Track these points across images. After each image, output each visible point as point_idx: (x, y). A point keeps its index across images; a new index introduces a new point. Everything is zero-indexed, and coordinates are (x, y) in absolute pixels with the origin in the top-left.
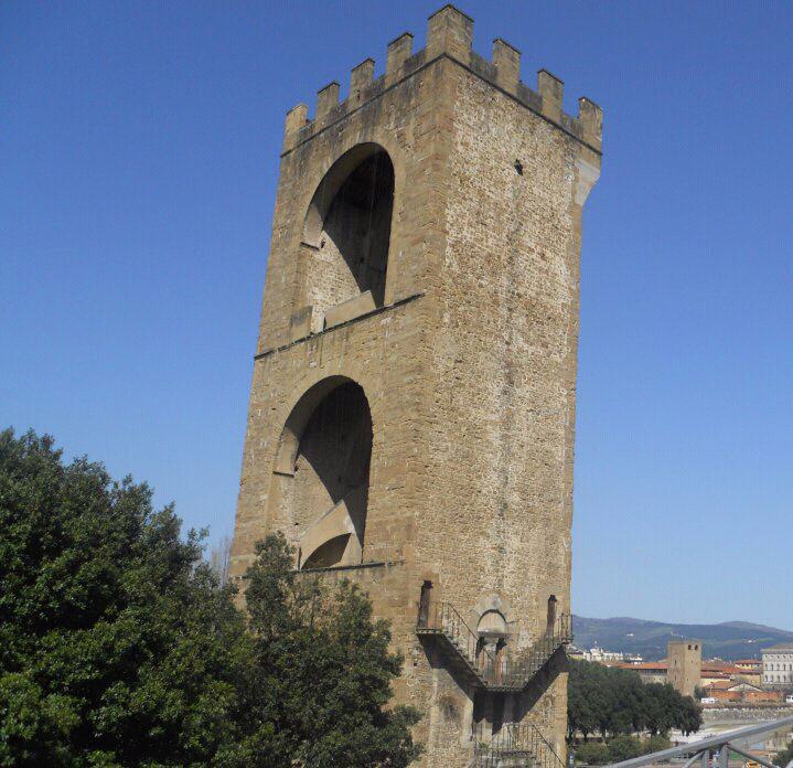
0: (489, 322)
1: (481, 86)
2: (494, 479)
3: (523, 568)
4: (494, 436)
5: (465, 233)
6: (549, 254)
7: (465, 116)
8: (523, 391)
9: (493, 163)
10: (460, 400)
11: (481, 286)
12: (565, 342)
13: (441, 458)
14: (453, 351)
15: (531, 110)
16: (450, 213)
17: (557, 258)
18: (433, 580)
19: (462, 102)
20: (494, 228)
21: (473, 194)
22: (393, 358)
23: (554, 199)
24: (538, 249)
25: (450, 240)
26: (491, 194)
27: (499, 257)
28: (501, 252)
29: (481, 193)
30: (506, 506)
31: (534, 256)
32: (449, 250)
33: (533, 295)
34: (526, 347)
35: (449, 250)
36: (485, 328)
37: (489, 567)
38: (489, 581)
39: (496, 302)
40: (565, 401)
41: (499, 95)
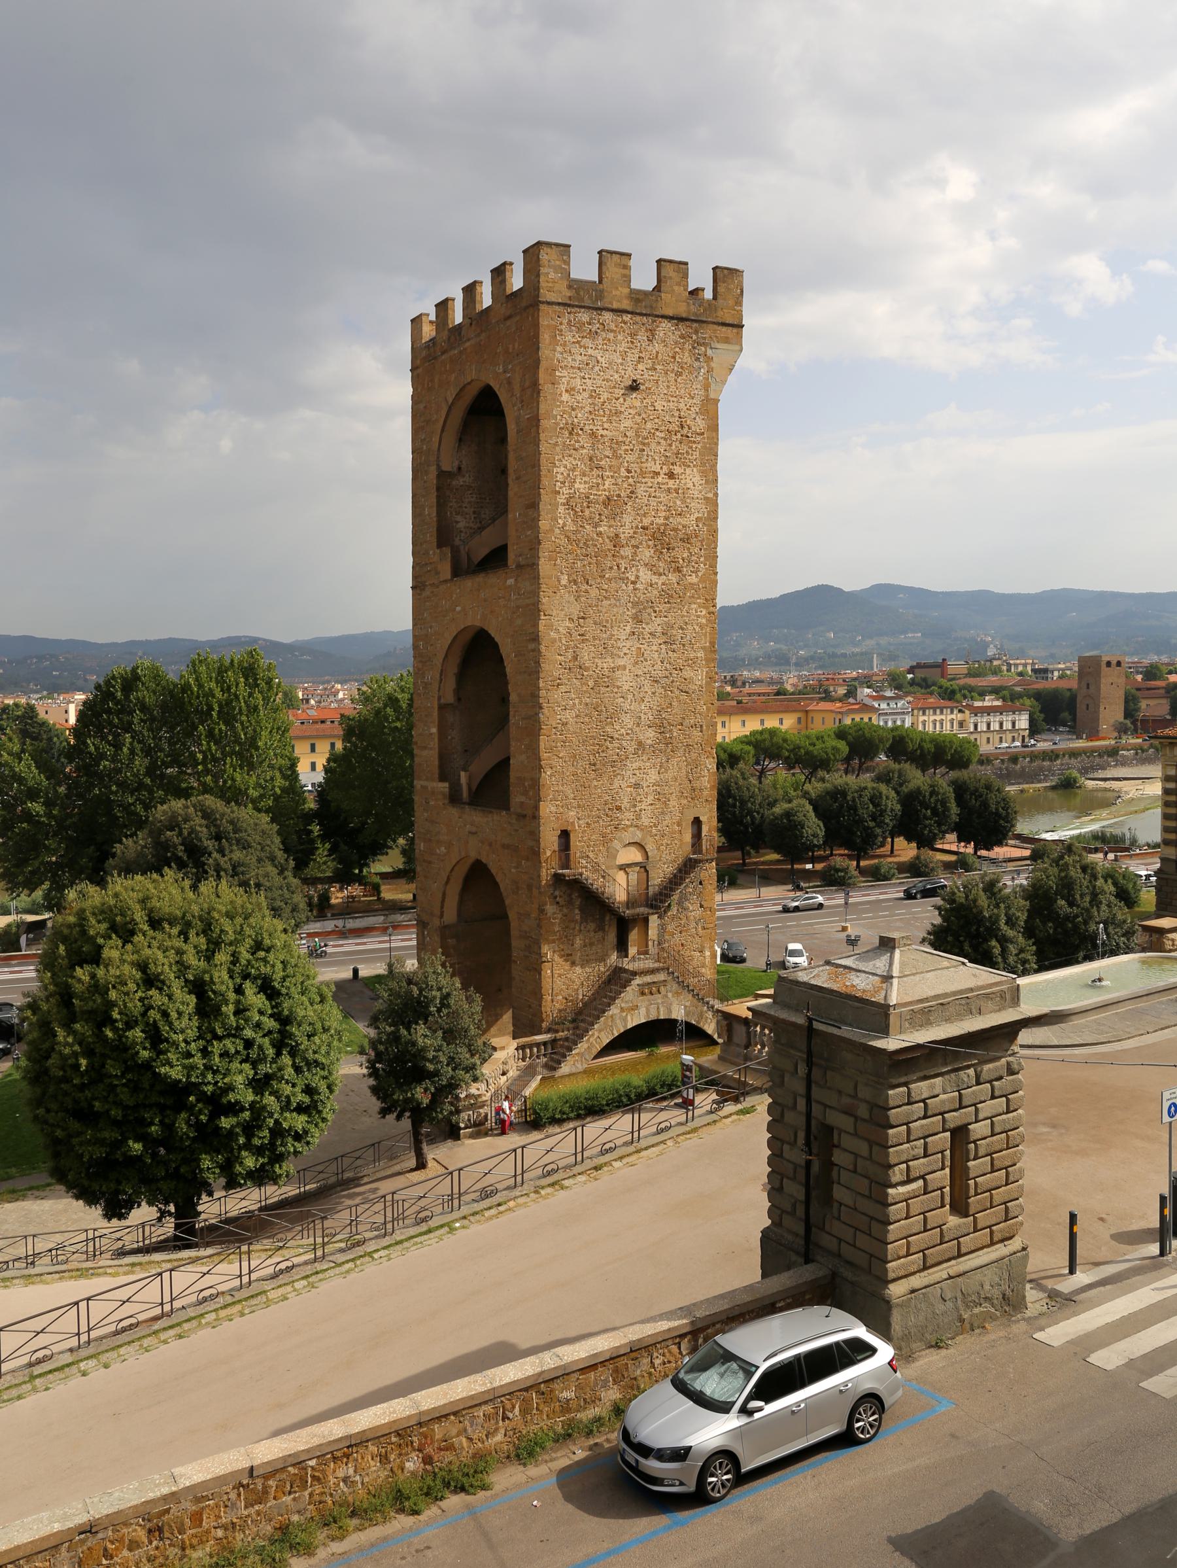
0: (611, 568)
1: (584, 316)
2: (628, 721)
3: (661, 798)
4: (625, 680)
5: (576, 486)
6: (677, 470)
7: (570, 359)
8: (656, 625)
9: (605, 396)
10: (586, 656)
11: (600, 534)
13: (569, 716)
14: (575, 610)
15: (645, 315)
17: (688, 471)
18: (569, 828)
19: (564, 345)
20: (610, 467)
21: (584, 440)
22: (519, 622)
23: (682, 406)
25: (561, 499)
27: (619, 496)
29: (593, 434)
30: (640, 744)
32: (561, 509)
33: (662, 521)
34: (655, 579)
35: (561, 509)
37: (625, 804)
38: (627, 817)
40: (704, 621)
41: (607, 316)
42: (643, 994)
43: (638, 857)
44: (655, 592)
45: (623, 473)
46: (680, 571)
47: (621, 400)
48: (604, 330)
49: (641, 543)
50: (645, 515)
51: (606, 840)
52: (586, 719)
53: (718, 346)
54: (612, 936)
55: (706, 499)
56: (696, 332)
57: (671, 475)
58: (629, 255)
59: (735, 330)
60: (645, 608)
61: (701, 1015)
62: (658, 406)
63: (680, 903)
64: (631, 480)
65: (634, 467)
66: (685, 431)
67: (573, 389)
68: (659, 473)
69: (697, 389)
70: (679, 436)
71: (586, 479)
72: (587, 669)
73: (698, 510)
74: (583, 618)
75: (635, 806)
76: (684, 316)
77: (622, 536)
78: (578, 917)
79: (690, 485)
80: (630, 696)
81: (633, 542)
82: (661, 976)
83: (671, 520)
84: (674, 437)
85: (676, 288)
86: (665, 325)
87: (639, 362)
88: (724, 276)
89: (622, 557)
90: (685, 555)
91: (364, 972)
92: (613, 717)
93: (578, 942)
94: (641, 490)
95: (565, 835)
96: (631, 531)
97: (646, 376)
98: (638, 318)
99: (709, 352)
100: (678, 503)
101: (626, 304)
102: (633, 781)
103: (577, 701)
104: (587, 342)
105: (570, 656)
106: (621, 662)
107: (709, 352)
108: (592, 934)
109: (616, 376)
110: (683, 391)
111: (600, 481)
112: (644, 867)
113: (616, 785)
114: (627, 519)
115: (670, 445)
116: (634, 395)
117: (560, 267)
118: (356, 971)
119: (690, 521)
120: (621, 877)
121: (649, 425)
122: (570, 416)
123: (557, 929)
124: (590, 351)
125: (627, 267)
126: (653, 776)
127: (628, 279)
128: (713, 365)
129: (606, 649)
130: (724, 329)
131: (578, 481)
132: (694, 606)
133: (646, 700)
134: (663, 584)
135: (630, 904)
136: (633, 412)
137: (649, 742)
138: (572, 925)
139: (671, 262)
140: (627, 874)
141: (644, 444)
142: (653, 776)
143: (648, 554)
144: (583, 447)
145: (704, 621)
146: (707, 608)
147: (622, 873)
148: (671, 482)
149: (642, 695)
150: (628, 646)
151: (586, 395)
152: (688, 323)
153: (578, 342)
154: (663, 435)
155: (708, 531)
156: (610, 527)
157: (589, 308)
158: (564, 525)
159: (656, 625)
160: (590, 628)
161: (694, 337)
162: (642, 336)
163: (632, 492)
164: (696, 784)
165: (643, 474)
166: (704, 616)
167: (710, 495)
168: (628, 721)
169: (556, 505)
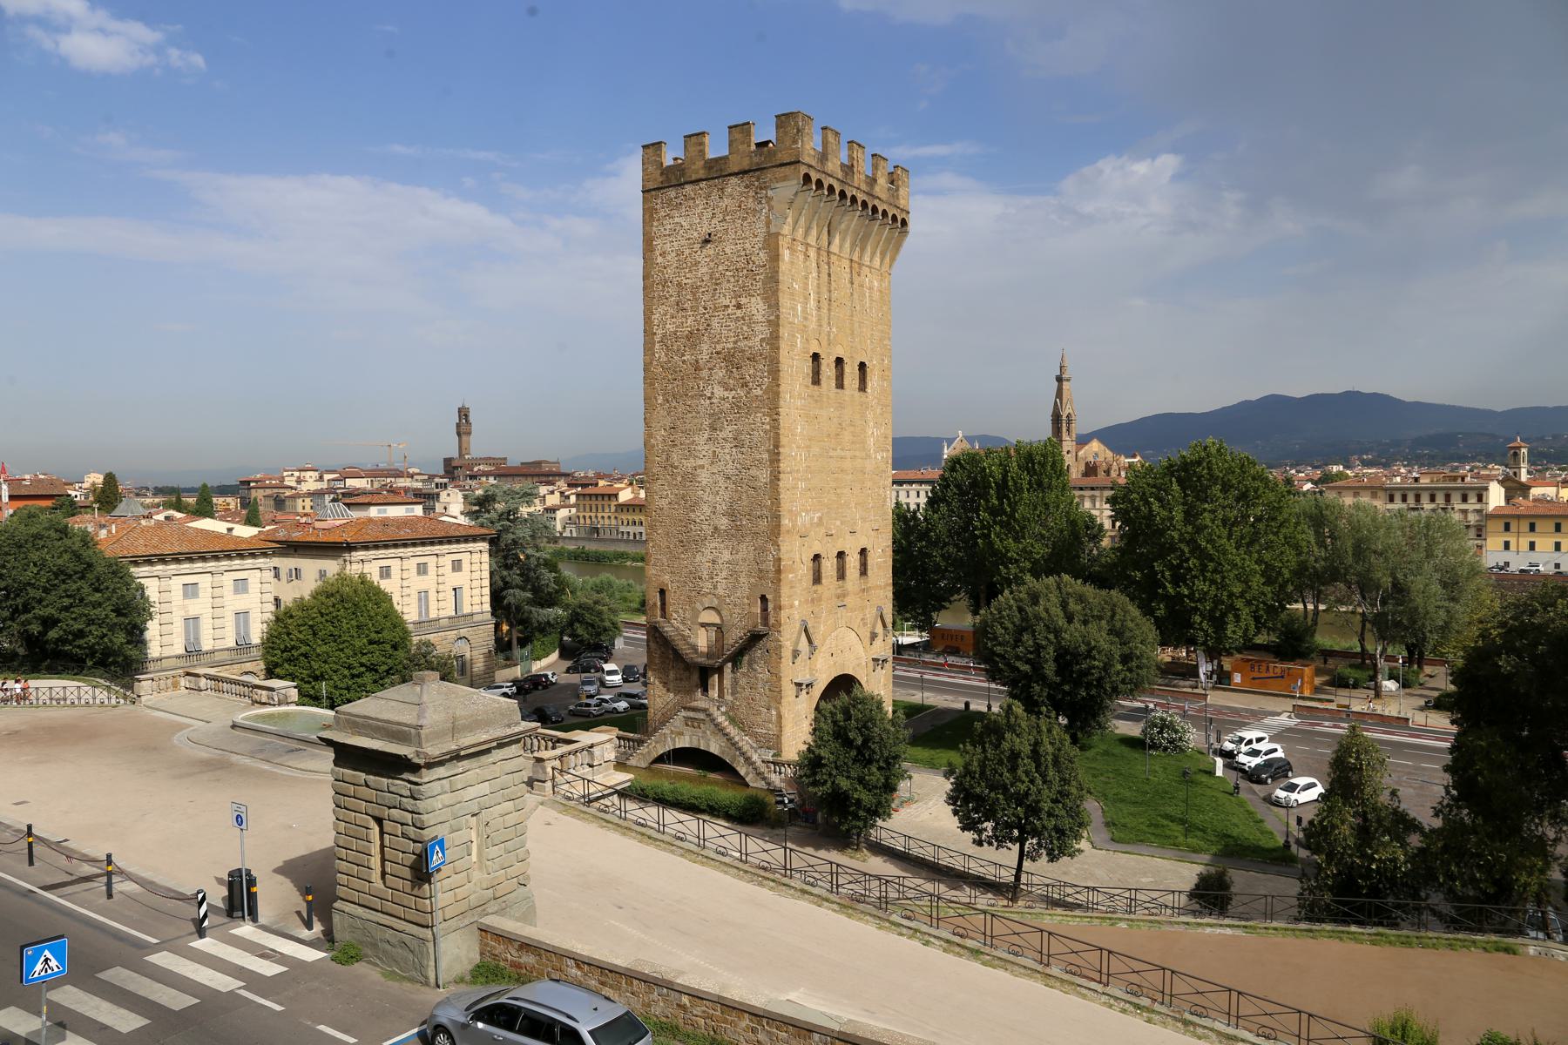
1: (672, 193)
2: (706, 509)
3: (734, 574)
4: (704, 477)
6: (743, 300)
8: (727, 432)
10: (675, 458)
13: (664, 503)
14: (668, 422)
16: (656, 317)
21: (672, 290)
29: (679, 285)
34: (726, 394)
35: (657, 346)
37: (705, 576)
39: (698, 369)
41: (688, 188)
43: (717, 620)
45: (702, 310)
51: (690, 601)
54: (696, 677)
57: (739, 306)
61: (734, 757)
62: (728, 250)
69: (760, 229)
73: (762, 331)
82: (702, 716)
86: (734, 180)
88: (784, 120)
91: (972, 707)
93: (672, 675)
94: (715, 323)
95: (662, 592)
99: (770, 193)
101: (702, 174)
106: (700, 462)
107: (770, 193)
112: (719, 628)
113: (698, 557)
114: (705, 347)
118: (967, 704)
120: (702, 632)
125: (702, 144)
126: (726, 556)
127: (702, 152)
129: (691, 453)
135: (709, 655)
142: (726, 556)
160: (678, 436)
162: (714, 196)
164: (763, 567)
168: (706, 509)
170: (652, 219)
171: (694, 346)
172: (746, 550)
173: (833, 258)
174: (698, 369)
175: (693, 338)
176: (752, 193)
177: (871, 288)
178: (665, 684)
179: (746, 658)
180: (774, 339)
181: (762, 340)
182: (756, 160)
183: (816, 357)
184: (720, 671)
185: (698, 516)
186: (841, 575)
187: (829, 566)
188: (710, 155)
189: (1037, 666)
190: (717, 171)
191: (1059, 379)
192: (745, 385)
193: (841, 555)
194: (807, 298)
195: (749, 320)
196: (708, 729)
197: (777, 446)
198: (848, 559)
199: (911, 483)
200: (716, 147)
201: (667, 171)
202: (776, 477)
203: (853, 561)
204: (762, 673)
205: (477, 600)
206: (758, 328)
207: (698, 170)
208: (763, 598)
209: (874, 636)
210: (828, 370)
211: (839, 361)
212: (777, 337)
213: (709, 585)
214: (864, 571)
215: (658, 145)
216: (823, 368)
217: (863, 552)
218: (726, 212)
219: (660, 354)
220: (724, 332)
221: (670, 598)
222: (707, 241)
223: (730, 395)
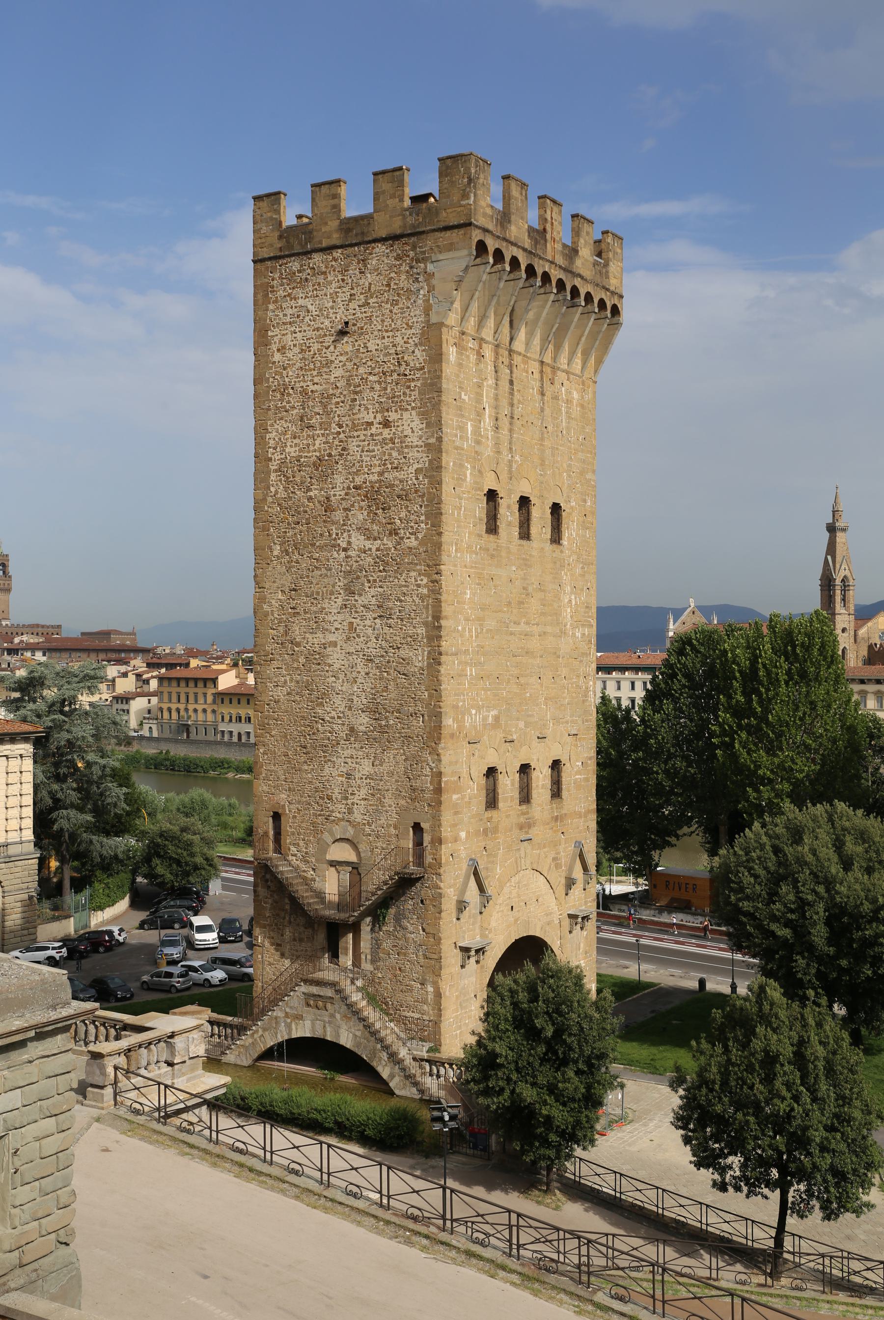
2: (339, 703)
3: (376, 794)
4: (336, 658)
6: (393, 416)
7: (281, 315)
8: (369, 596)
9: (315, 347)
10: (297, 631)
11: (310, 499)
12: (423, 518)
13: (280, 693)
14: (287, 581)
15: (356, 245)
16: (272, 437)
17: (406, 415)
18: (280, 811)
19: (276, 301)
21: (295, 400)
23: (399, 340)
24: (379, 417)
25: (273, 466)
26: (316, 387)
27: (330, 455)
28: (330, 448)
29: (304, 392)
30: (352, 729)
31: (373, 430)
33: (375, 478)
34: (368, 544)
35: (273, 477)
36: (318, 544)
37: (336, 795)
38: (338, 809)
39: (329, 509)
40: (425, 591)
41: (317, 258)
42: (308, 1005)
43: (352, 857)
44: (369, 559)
46: (396, 534)
47: (332, 348)
48: (314, 275)
49: (353, 506)
50: (357, 473)
51: (316, 830)
52: (297, 698)
53: (441, 257)
54: (321, 937)
55: (427, 445)
56: (414, 248)
57: (386, 424)
58: (337, 182)
59: (462, 231)
60: (358, 578)
61: (374, 1053)
62: (371, 346)
63: (397, 920)
64: (342, 436)
65: (346, 420)
66: (402, 369)
67: (284, 347)
68: (372, 424)
69: (417, 316)
70: (395, 376)
71: (296, 441)
72: (298, 645)
73: (419, 458)
74: (295, 590)
75: (346, 798)
76: (398, 232)
77: (332, 498)
78: (288, 907)
79: (408, 432)
80: (341, 676)
81: (344, 504)
82: (329, 992)
83: (386, 475)
84: (389, 379)
85: (390, 202)
86: (380, 248)
87: (350, 300)
89: (333, 523)
90: (403, 515)
91: (710, 986)
92: (322, 698)
93: (288, 933)
94: (353, 446)
95: (277, 817)
96: (343, 493)
97: (359, 315)
98: (349, 250)
99: (430, 267)
100: (395, 454)
102: (345, 770)
103: (288, 678)
104: (299, 293)
105: (281, 629)
106: (331, 638)
107: (430, 267)
108: (302, 929)
109: (327, 323)
110: (399, 322)
111: (310, 441)
112: (355, 868)
113: (327, 771)
114: (339, 479)
115: (386, 389)
116: (346, 339)
117: (271, 218)
118: (702, 983)
119: (409, 473)
121: (361, 370)
122: (282, 377)
123: (267, 915)
124: (301, 302)
125: (336, 196)
126: (366, 767)
127: (336, 208)
128: (434, 282)
129: (318, 624)
130: (448, 234)
131: (288, 444)
132: (413, 574)
133: (359, 681)
134: (378, 550)
135: (340, 906)
136: (343, 358)
137: (362, 728)
138: (282, 914)
139: (384, 172)
140: (339, 872)
141: (356, 393)
142: (366, 767)
143: (361, 517)
144: (293, 407)
145: (425, 591)
146: (428, 575)
147: (333, 869)
148: (387, 431)
149: (354, 674)
150: (337, 618)
151: (297, 350)
152: (404, 240)
153: (289, 295)
154: (375, 378)
155: (430, 483)
156: (321, 490)
157: (298, 254)
158: (276, 492)
159: (369, 596)
160: (302, 602)
161: (412, 254)
163: (344, 449)
164: (417, 784)
165: (354, 427)
166: (425, 586)
167: (432, 441)
168: (339, 703)
169: (268, 473)
170: (266, 300)
171: (324, 478)
172: (393, 760)
173: (517, 359)
174: (329, 509)
175: (322, 467)
176: (405, 268)
177: (568, 401)
178: (278, 946)
179: (392, 911)
180: (434, 470)
181: (418, 471)
182: (410, 220)
183: (492, 495)
184: (355, 928)
185: (327, 711)
186: (525, 797)
187: (508, 784)
188: (349, 211)
189: (800, 931)
190: (357, 236)
191: (832, 529)
192: (394, 532)
193: (525, 769)
194: (480, 414)
195: (400, 443)
196: (338, 1011)
197: (437, 617)
198: (535, 775)
199: (623, 669)
200: (356, 203)
201: (287, 234)
202: (435, 660)
203: (541, 778)
204: (415, 932)
205: (14, 824)
206: (412, 454)
207: (330, 233)
208: (417, 828)
209: (570, 883)
210: (508, 514)
211: (524, 502)
212: (439, 468)
213: (341, 807)
214: (556, 792)
215: (274, 197)
216: (502, 511)
217: (556, 765)
218: (369, 292)
219: (277, 487)
220: (365, 459)
221: (288, 826)
222: (342, 333)
223: (374, 545)
